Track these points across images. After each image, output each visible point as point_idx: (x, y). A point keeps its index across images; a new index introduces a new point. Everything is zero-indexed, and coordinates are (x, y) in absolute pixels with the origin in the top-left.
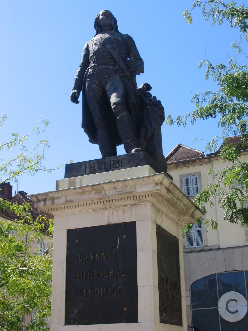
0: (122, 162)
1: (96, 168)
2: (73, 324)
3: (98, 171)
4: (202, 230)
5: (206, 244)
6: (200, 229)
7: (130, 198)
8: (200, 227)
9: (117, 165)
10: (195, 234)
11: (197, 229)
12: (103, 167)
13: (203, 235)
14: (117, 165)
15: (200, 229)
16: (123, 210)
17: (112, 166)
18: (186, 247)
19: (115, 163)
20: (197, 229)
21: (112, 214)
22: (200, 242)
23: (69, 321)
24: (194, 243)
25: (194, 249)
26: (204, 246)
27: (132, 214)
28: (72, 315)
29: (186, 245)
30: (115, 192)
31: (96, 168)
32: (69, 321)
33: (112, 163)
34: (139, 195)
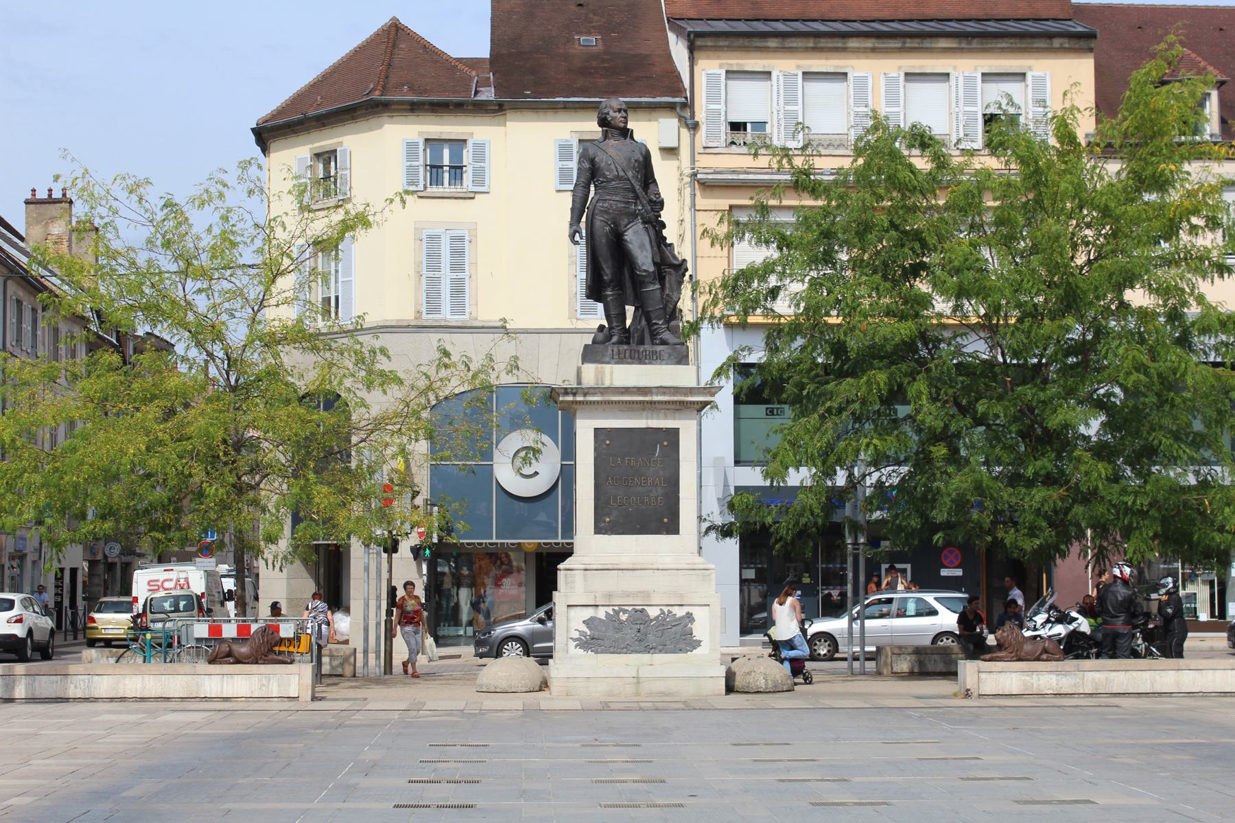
1: (627, 355)
2: (605, 533)
4: (467, 278)
5: (474, 314)
6: (461, 275)
8: (463, 271)
10: (448, 286)
11: (454, 276)
13: (467, 290)
15: (461, 275)
18: (424, 316)
20: (454, 276)
22: (458, 308)
23: (598, 530)
24: (443, 308)
25: (443, 323)
26: (467, 317)
28: (603, 525)
29: (424, 310)
31: (627, 355)
32: (598, 530)
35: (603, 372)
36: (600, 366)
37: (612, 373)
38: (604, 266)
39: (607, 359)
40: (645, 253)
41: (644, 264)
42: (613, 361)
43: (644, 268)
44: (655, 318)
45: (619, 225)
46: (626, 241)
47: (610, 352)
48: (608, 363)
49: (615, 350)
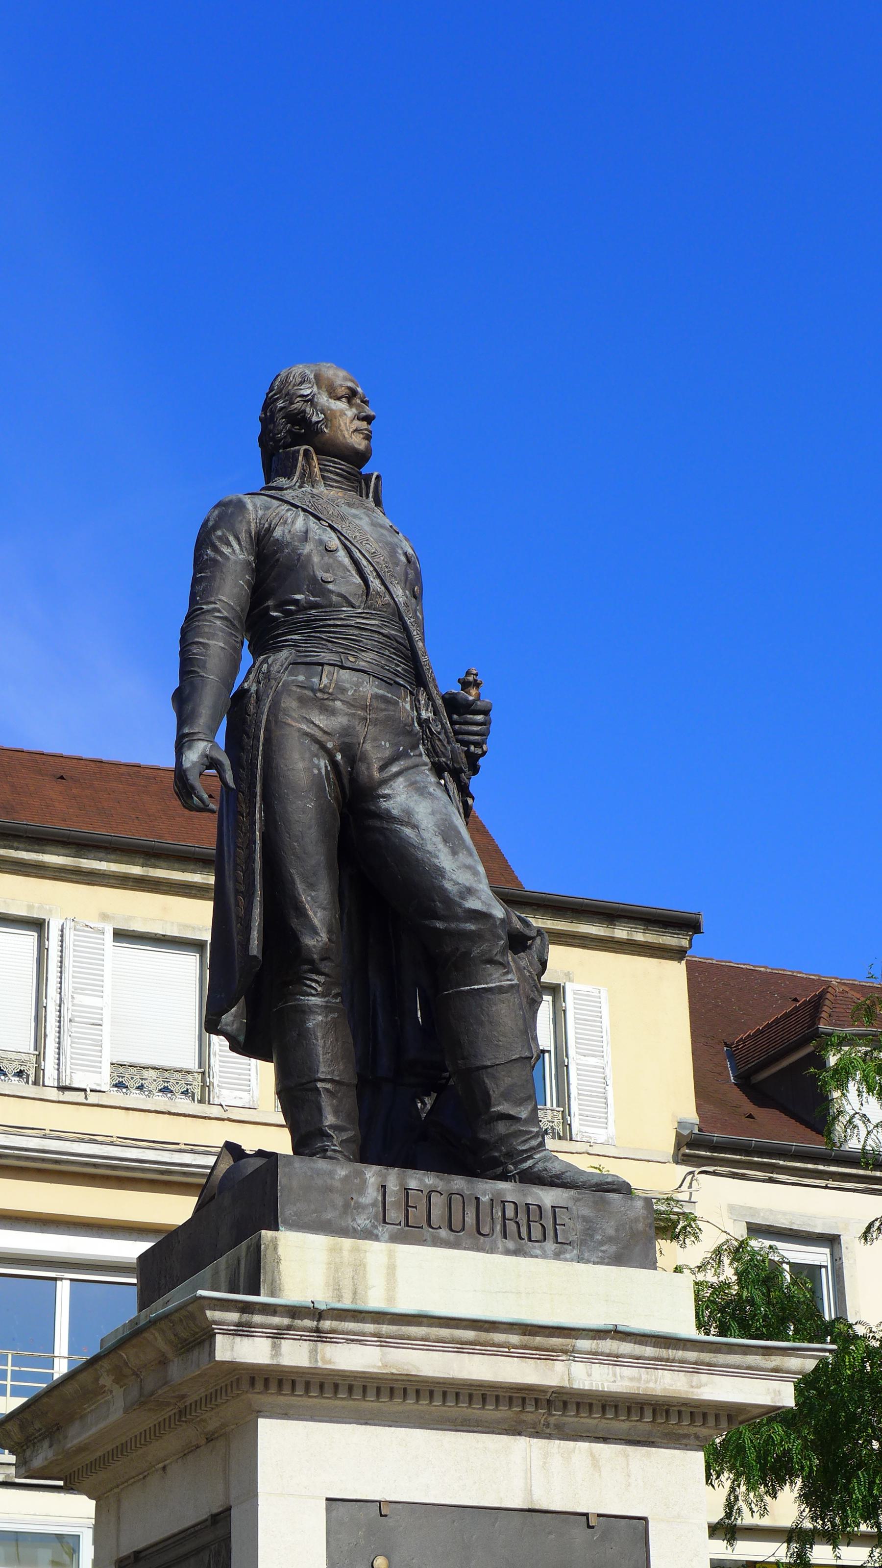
0: (555, 1223)
1: (436, 1213)
3: (444, 1233)
7: (642, 1409)
9: (536, 1233)
12: (470, 1219)
14: (536, 1233)
16: (592, 1455)
17: (511, 1227)
19: (522, 1218)
21: (545, 1463)
27: (629, 1485)
30: (615, 1375)
33: (510, 1213)
34: (683, 1409)
35: (359, 1268)
36: (347, 1243)
37: (391, 1269)
38: (304, 898)
39: (362, 1221)
40: (463, 857)
41: (469, 891)
42: (384, 1231)
43: (473, 904)
44: (506, 1096)
45: (364, 758)
46: (387, 816)
47: (372, 1194)
48: (369, 1235)
49: (393, 1185)
